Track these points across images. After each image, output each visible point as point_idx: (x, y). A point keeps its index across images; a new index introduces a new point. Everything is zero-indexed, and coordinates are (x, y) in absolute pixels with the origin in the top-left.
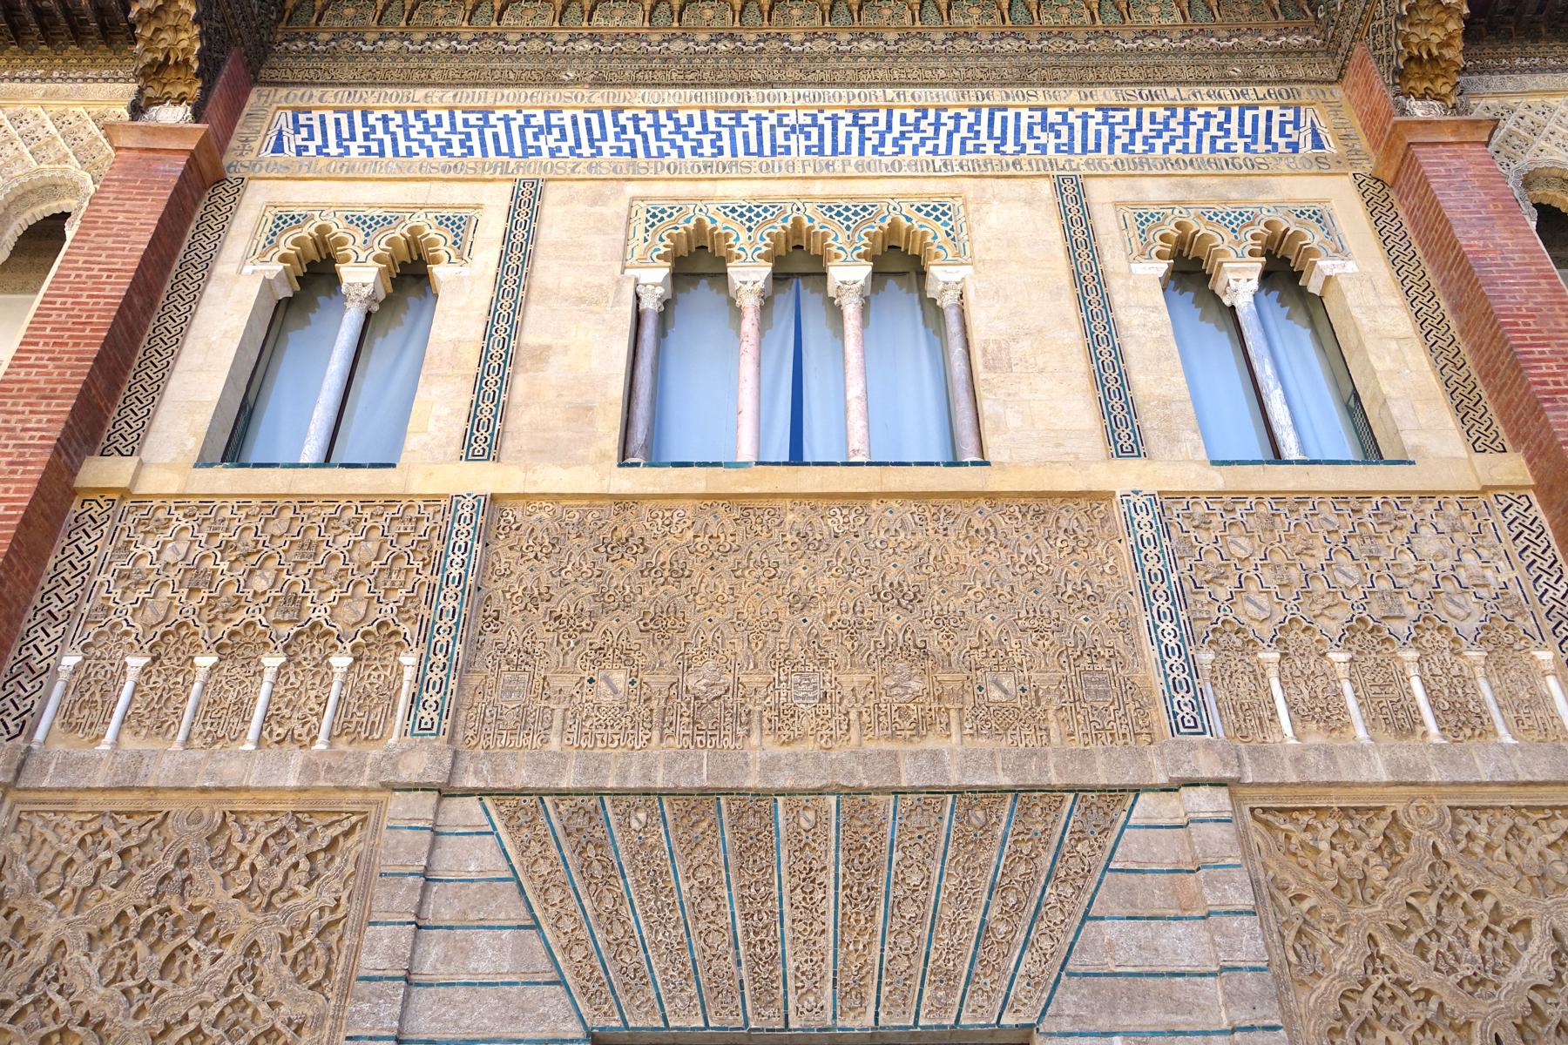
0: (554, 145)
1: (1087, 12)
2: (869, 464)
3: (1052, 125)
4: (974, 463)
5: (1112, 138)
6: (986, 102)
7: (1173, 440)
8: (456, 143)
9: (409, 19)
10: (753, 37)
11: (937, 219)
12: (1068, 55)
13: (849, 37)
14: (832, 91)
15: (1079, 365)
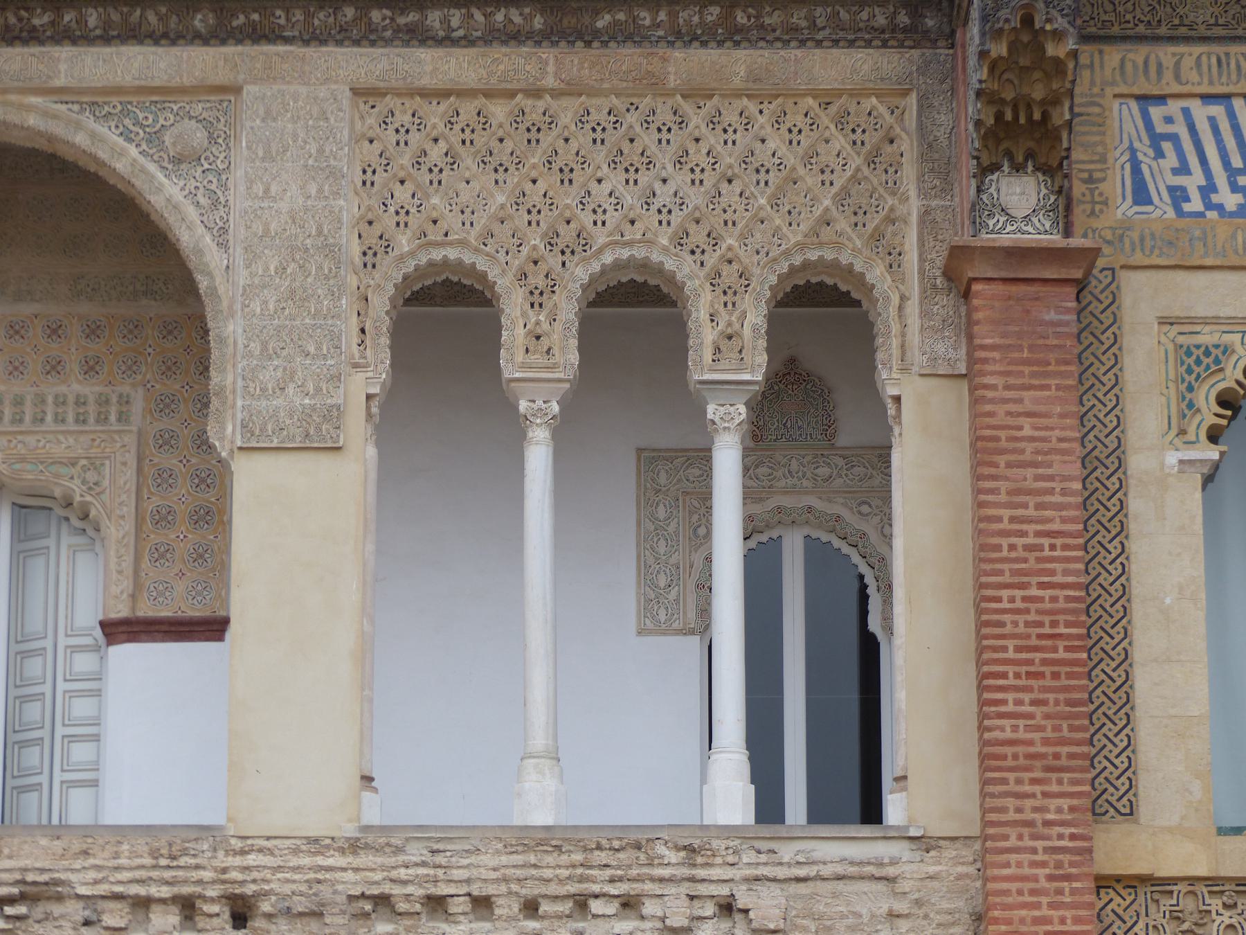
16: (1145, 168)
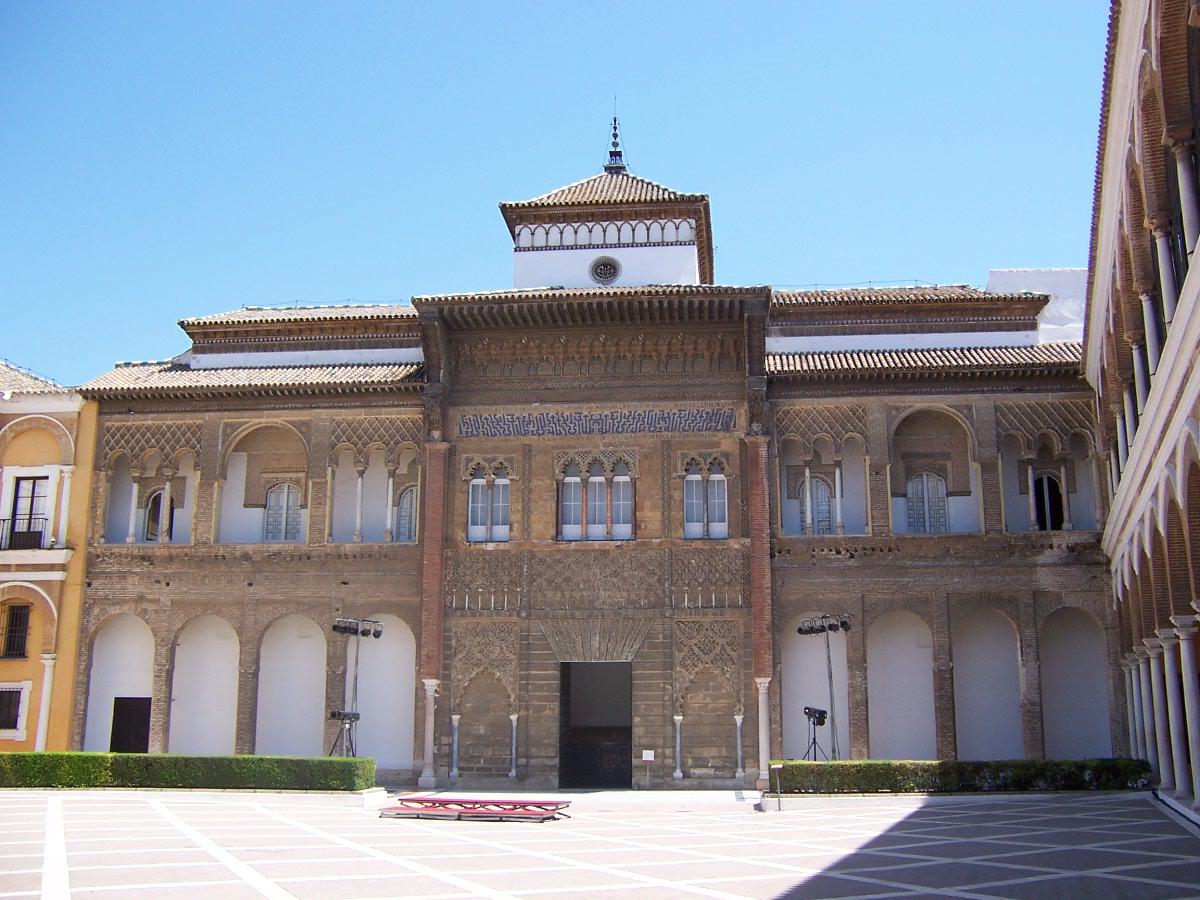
5: (680, 423)
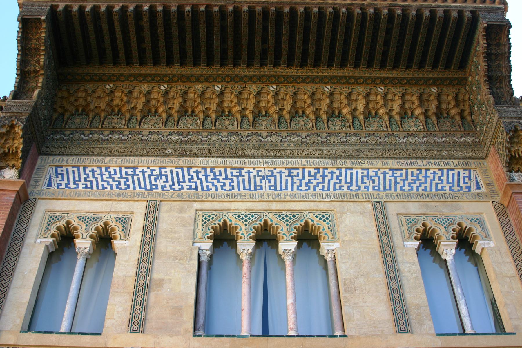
0: (163, 184)
1: (384, 124)
2: (298, 336)
3: (371, 177)
4: (340, 336)
5: (396, 183)
6: (344, 166)
7: (421, 324)
8: (122, 183)
9: (103, 124)
10: (246, 134)
11: (324, 221)
12: (377, 144)
13: (286, 134)
14: (279, 160)
15: (384, 290)
16: (52, 180)
